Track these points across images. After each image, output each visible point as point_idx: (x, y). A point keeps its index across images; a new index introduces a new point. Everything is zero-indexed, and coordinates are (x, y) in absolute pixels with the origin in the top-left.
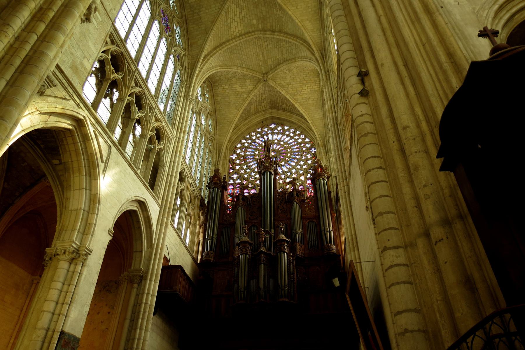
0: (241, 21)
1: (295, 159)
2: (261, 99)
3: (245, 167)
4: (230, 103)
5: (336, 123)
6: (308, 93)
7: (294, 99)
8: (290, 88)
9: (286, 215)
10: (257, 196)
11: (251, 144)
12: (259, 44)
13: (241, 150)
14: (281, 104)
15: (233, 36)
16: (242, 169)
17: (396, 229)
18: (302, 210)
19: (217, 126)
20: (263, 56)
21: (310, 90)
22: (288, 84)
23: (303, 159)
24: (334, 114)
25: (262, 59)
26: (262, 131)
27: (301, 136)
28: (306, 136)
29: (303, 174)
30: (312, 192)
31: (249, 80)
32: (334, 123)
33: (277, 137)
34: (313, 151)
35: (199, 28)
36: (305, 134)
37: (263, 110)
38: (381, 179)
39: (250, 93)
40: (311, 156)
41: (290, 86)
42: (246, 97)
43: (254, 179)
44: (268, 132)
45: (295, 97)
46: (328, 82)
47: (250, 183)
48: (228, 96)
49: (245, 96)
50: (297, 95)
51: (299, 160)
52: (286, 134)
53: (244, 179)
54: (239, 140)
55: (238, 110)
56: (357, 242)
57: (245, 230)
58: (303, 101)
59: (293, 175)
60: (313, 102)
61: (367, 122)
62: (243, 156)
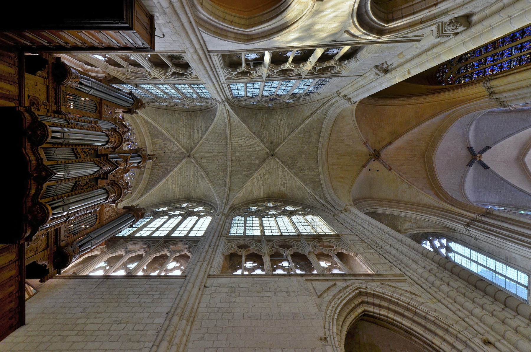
12: (219, 155)
14: (159, 165)
20: (208, 157)
22: (181, 173)
25: (206, 155)
31: (188, 142)
41: (180, 175)
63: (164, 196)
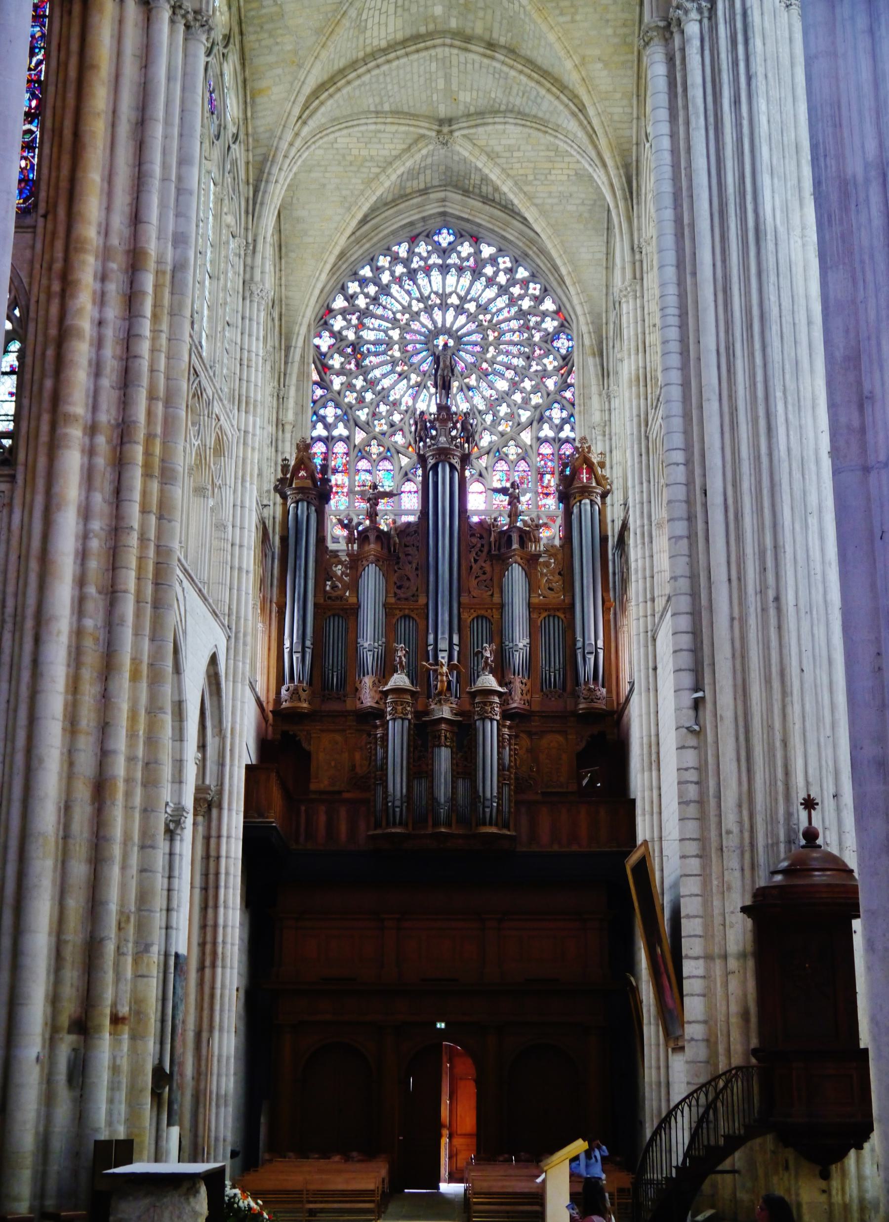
0: (399, 10)
1: (507, 369)
2: (417, 167)
3: (359, 383)
4: (324, 185)
5: (646, 432)
6: (569, 180)
7: (525, 193)
8: (515, 160)
9: (490, 593)
10: (416, 532)
11: (375, 300)
13: (345, 319)
14: (478, 182)
15: (369, 50)
16: (350, 387)
17: (700, 936)
18: (532, 586)
19: (280, 258)
20: (447, 78)
21: (576, 174)
22: (510, 149)
23: (533, 369)
24: (642, 401)
26: (411, 252)
27: (531, 285)
28: (546, 290)
29: (531, 424)
30: (552, 484)
32: (640, 431)
33: (458, 281)
34: (562, 344)
35: (277, 43)
36: (543, 281)
37: (419, 191)
38: (695, 872)
39: (391, 163)
40: (556, 364)
41: (515, 154)
42: (377, 176)
43: (385, 428)
44: (430, 262)
45: (526, 189)
46: (638, 288)
47: (375, 438)
48: (319, 165)
49: (377, 170)
50: (535, 182)
51: (522, 373)
52: (485, 275)
53: (356, 425)
54: (339, 286)
55: (349, 209)
56: (658, 753)
57: (400, 657)
58: (550, 201)
59: (499, 424)
60: (581, 208)
61: (691, 782)
62: (353, 345)
63: (586, 215)
